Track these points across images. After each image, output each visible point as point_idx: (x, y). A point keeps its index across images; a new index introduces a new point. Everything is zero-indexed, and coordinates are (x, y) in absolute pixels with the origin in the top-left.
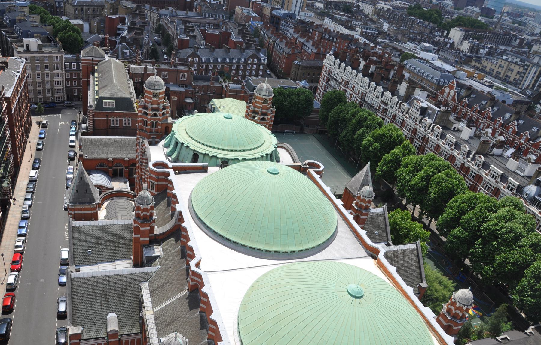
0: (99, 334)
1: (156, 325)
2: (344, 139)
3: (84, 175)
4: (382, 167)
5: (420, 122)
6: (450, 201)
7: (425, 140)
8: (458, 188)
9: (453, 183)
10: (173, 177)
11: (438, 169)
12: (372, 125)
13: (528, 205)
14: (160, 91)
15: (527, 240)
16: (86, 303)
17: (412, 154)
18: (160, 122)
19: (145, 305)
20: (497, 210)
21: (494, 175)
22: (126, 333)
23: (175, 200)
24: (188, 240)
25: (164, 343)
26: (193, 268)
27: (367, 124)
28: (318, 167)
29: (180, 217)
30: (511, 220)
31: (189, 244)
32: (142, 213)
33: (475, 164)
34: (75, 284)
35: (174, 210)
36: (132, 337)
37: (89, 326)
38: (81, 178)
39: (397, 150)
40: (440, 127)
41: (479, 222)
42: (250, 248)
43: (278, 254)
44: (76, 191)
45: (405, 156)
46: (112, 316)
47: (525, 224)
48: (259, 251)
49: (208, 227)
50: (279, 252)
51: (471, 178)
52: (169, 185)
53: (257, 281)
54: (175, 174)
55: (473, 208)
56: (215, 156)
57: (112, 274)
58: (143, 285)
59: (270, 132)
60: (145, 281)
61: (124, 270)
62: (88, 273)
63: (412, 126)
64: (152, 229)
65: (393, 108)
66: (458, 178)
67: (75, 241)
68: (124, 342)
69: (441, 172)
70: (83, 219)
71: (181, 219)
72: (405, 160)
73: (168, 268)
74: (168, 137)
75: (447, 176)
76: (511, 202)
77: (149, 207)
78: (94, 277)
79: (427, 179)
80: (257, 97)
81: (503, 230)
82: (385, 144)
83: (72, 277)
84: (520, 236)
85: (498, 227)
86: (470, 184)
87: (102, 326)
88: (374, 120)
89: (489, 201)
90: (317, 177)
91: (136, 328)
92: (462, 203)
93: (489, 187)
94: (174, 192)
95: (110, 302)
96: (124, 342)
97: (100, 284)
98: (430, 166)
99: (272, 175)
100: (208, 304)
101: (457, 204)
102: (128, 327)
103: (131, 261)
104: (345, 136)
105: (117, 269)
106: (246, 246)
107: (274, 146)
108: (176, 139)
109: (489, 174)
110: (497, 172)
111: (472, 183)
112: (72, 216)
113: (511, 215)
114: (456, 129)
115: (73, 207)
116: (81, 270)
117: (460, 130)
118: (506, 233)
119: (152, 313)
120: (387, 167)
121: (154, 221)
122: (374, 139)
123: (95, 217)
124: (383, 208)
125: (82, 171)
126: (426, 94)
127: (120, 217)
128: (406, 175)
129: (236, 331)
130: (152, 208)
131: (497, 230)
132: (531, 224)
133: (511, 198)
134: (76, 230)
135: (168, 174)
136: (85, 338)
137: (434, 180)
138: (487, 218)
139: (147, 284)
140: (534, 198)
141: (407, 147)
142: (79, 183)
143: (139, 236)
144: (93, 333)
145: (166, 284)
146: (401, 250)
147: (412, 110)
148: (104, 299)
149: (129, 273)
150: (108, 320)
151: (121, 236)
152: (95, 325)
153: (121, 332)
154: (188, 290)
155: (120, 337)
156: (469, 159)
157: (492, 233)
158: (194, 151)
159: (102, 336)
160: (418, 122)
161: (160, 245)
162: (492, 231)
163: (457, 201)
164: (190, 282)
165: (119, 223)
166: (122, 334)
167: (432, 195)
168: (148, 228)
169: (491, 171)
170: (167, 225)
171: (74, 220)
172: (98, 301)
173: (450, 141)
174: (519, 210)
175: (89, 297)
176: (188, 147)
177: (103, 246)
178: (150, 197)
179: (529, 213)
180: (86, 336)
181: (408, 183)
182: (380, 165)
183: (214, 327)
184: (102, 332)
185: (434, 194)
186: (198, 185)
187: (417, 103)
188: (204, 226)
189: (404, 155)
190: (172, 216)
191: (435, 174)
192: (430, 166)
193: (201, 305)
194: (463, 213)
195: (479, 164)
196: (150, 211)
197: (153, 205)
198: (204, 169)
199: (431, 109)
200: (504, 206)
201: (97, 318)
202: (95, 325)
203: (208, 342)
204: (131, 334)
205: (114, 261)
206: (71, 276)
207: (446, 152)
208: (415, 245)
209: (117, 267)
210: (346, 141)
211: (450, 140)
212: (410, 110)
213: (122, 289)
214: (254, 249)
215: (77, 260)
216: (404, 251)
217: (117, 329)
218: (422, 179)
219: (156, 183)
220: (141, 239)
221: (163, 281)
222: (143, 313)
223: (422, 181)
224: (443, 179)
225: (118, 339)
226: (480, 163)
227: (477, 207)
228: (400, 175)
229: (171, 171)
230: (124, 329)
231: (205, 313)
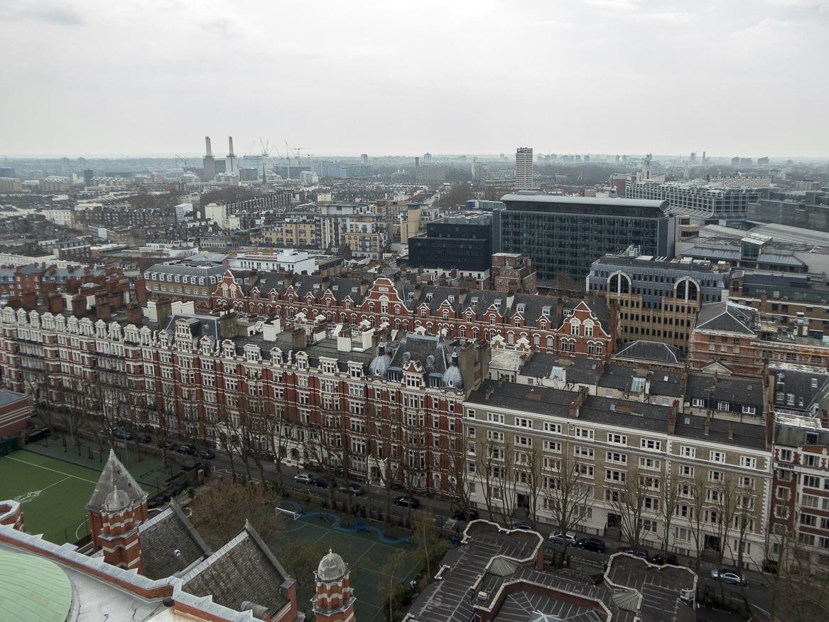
21: (329, 368)
65: (148, 345)
86: (307, 395)
111: (309, 393)
114: (254, 333)
124: (170, 506)
146: (225, 555)
156: (289, 363)
199: (206, 321)
208: (245, 533)
216: (231, 553)
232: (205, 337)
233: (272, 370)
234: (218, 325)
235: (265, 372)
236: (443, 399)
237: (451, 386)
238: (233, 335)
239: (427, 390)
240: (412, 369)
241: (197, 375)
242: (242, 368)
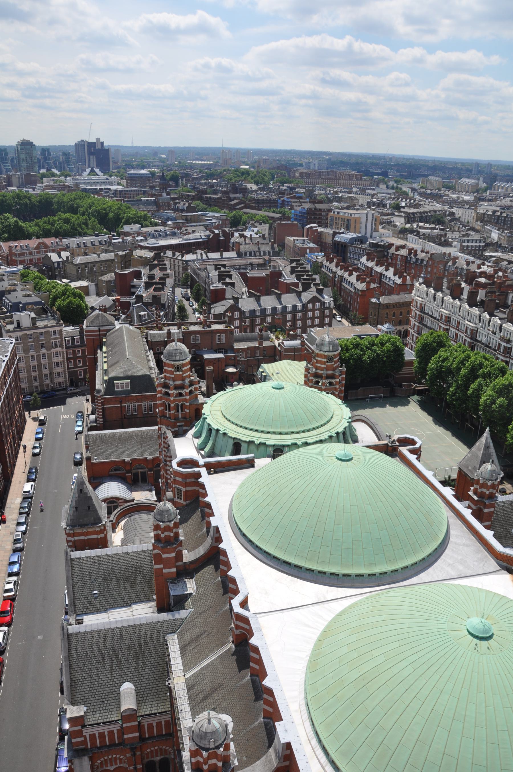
0: (109, 716)
1: (190, 698)
2: (454, 397)
3: (84, 486)
10: (205, 478)
12: (490, 373)
14: (184, 362)
16: (90, 670)
18: (188, 404)
19: (173, 668)
22: (148, 713)
23: (210, 511)
24: (229, 568)
25: (193, 729)
26: (237, 609)
27: (484, 372)
28: (413, 442)
29: (217, 535)
31: (231, 573)
32: (163, 533)
34: (74, 643)
35: (209, 523)
36: (157, 719)
37: (95, 704)
38: (81, 490)
42: (319, 572)
43: (361, 578)
44: (75, 509)
46: (127, 687)
48: (332, 576)
49: (257, 546)
50: (363, 575)
52: (201, 491)
53: (331, 623)
54: (209, 474)
56: (264, 444)
57: (125, 624)
58: (170, 638)
59: (339, 401)
60: (173, 633)
61: (142, 618)
62: (98, 624)
64: (179, 556)
67: (76, 580)
68: (146, 726)
70: (87, 548)
71: (218, 539)
73: (204, 611)
74: (198, 424)
77: (171, 524)
78: (101, 631)
80: (318, 355)
83: (70, 632)
87: (113, 704)
88: (493, 366)
90: (412, 458)
91: (163, 704)
94: (207, 499)
95: (124, 665)
96: (146, 726)
97: (109, 640)
99: (343, 463)
100: (260, 662)
102: (151, 703)
103: (154, 604)
104: (454, 394)
105: (135, 617)
106: (313, 571)
107: (347, 421)
108: (209, 425)
112: (70, 544)
115: (71, 532)
116: (84, 620)
119: (183, 680)
121: (181, 543)
122: (497, 392)
123: (104, 543)
125: (82, 480)
127: (137, 541)
129: (303, 702)
130: (176, 525)
134: (76, 563)
135: (199, 475)
136: (90, 723)
139: (176, 636)
142: (79, 497)
143: (161, 566)
144: (101, 715)
145: (202, 635)
148: (115, 663)
149: (149, 622)
150: (122, 694)
151: (139, 568)
152: (103, 702)
153: (141, 711)
154: (233, 642)
155: (139, 719)
158: (234, 438)
159: (113, 719)
161: (192, 578)
164: (235, 630)
165: (135, 550)
166: (143, 714)
168: (173, 555)
170: (201, 547)
171: (74, 549)
172: (107, 665)
175: (94, 661)
176: (225, 434)
177: (114, 584)
178: (172, 510)
180: (91, 720)
183: (271, 699)
184: (113, 713)
186: (241, 486)
188: (251, 546)
190: (208, 532)
193: (252, 664)
196: (174, 530)
197: (178, 521)
198: (250, 464)
201: (105, 692)
202: (103, 702)
203: (264, 722)
204: (156, 714)
205: (130, 606)
206: (67, 630)
209: (135, 613)
210: (457, 400)
213: (140, 646)
214: (325, 573)
215: (78, 607)
217: (134, 707)
219: (183, 489)
220: (165, 571)
221: (197, 631)
222: (170, 681)
225: (136, 723)
229: (203, 471)
230: (145, 707)
231: (257, 676)
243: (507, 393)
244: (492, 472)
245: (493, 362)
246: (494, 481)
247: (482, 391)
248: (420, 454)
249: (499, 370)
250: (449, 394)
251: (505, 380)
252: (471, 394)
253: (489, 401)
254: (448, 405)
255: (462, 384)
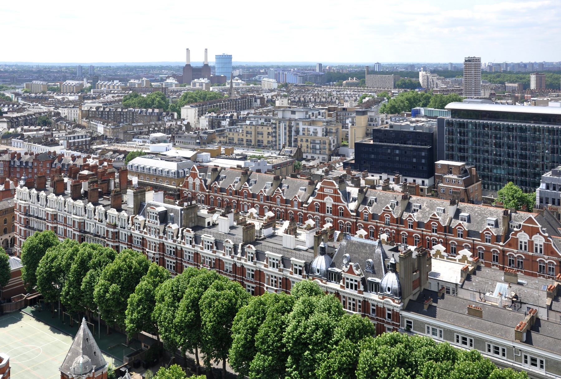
2: (68, 297)
4: (132, 316)
5: (165, 232)
6: (233, 323)
7: (179, 253)
8: (237, 300)
9: (228, 296)
11: (203, 285)
12: (100, 262)
13: (326, 284)
15: (339, 329)
17: (165, 280)
20: (291, 307)
21: (274, 263)
27: (94, 262)
30: (311, 312)
33: (247, 259)
39: (144, 283)
40: (191, 230)
41: (278, 334)
45: (157, 285)
47: (329, 310)
51: (250, 279)
55: (264, 318)
63: (156, 241)
65: (124, 228)
66: (232, 286)
69: (208, 287)
72: (159, 292)
75: (217, 290)
76: (303, 289)
79: (194, 305)
81: (308, 330)
82: (125, 281)
84: (330, 328)
85: (300, 330)
86: (253, 288)
88: (102, 254)
89: (277, 299)
92: (248, 318)
93: (275, 281)
98: (192, 285)
101: (242, 322)
104: (67, 293)
109: (269, 264)
110: (275, 258)
111: (254, 286)
113: (308, 305)
114: (211, 225)
117: (217, 223)
118: (314, 331)
120: (139, 312)
122: (109, 280)
126: (161, 194)
128: (165, 313)
131: (301, 334)
132: (335, 306)
133: (301, 283)
137: (202, 303)
138: (285, 324)
140: (327, 271)
141: (156, 274)
147: (149, 222)
156: (239, 255)
157: (299, 341)
160: (161, 235)
162: (297, 338)
163: (241, 318)
167: (209, 325)
169: (269, 260)
173: (208, 242)
174: (316, 294)
179: (331, 293)
181: (172, 323)
182: (128, 314)
185: (210, 322)
187: (152, 210)
189: (155, 285)
191: (202, 294)
192: (192, 285)
194: (254, 331)
195: (252, 257)
199: (172, 211)
200: (298, 297)
207: (210, 258)
210: (71, 299)
211: (207, 240)
212: (147, 222)
218: (187, 308)
223: (189, 311)
224: (213, 296)
226: (252, 256)
227: (268, 315)
228: (159, 316)
232: (170, 224)
233: (224, 260)
234: (181, 214)
235: (218, 262)
236: (380, 305)
237: (389, 293)
238: (193, 225)
239: (366, 295)
240: (351, 271)
241: (161, 259)
242: (199, 256)
243: (118, 277)
244: (85, 364)
245: (101, 250)
246: (89, 374)
247: (94, 282)
248: (9, 371)
249: (108, 256)
250: (62, 295)
251: (114, 265)
252: (84, 289)
253: (102, 291)
254: (64, 308)
255: (74, 281)
